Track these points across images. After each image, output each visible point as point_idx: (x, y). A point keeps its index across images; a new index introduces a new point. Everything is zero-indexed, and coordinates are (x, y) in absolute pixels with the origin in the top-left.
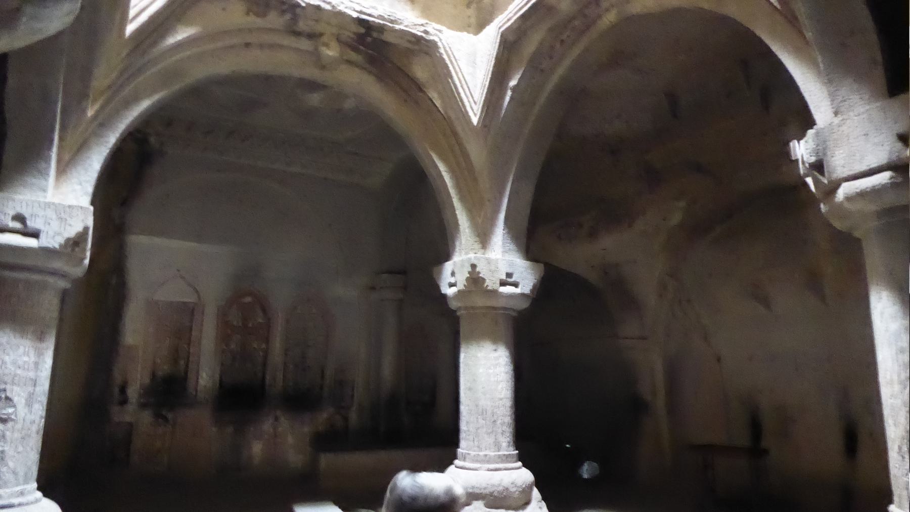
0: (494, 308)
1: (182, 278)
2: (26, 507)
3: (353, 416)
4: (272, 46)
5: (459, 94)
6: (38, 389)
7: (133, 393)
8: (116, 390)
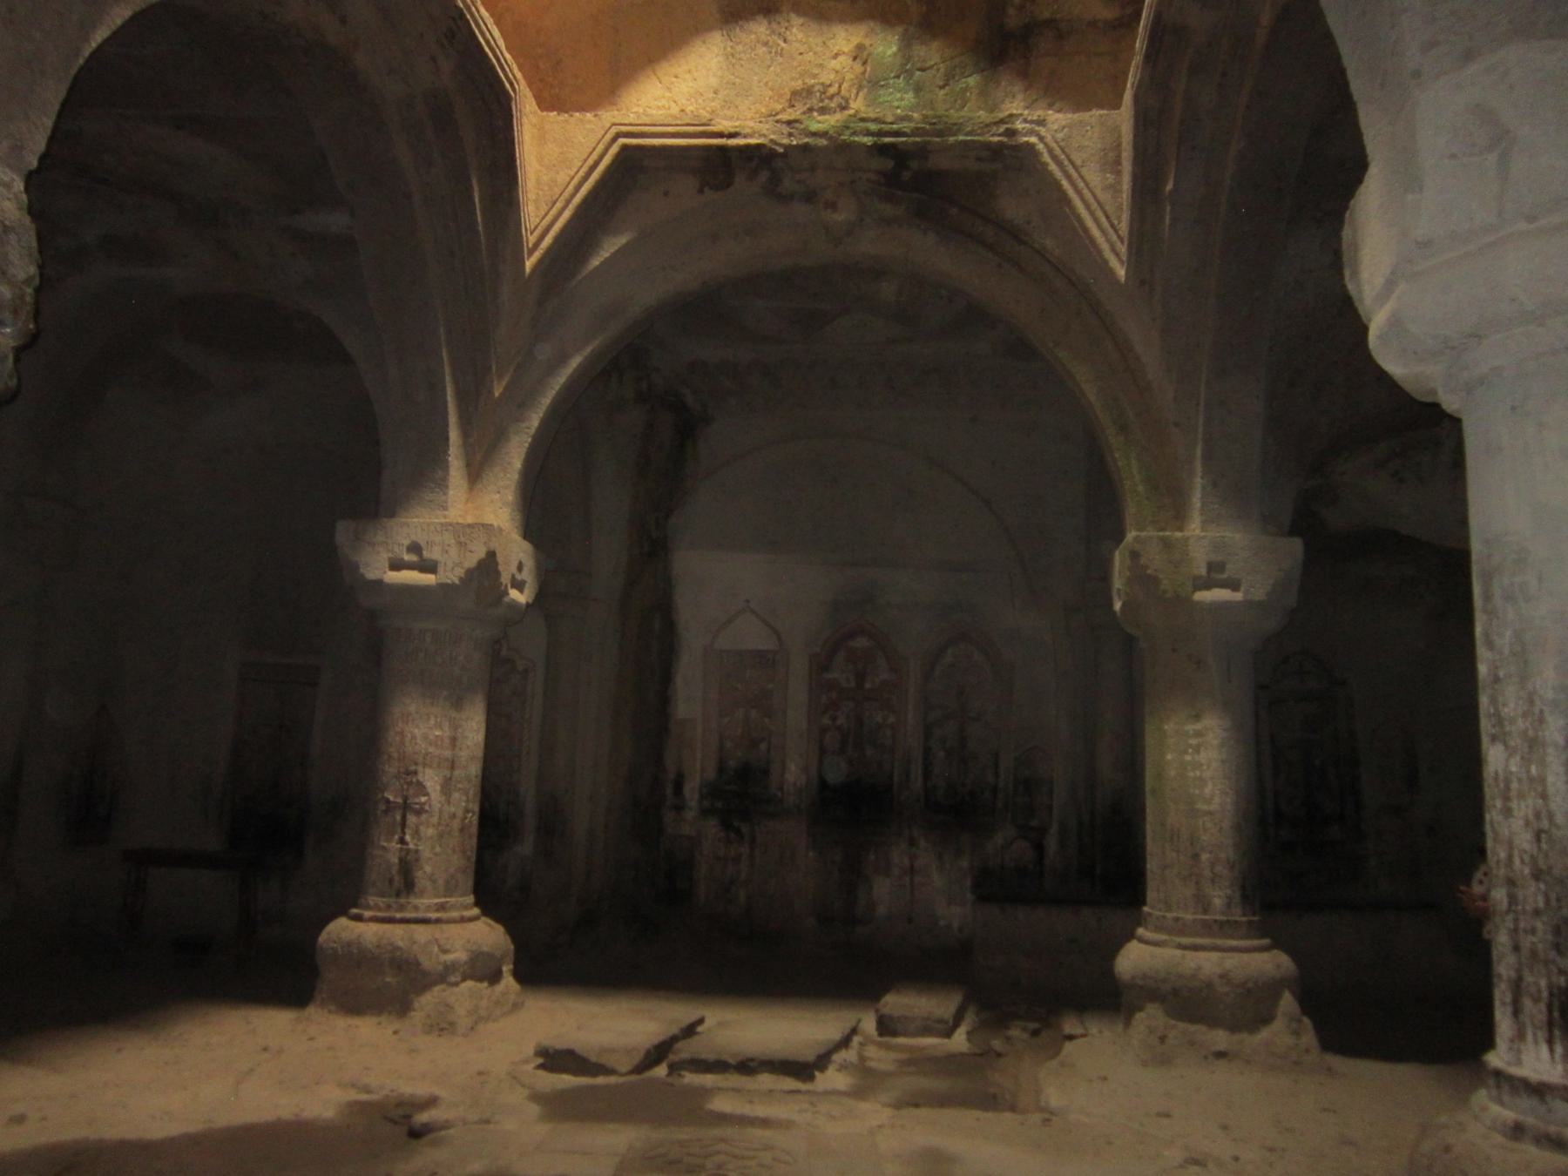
1: (753, 612)
2: (445, 927)
5: (1086, 230)
6: (457, 773)
7: (691, 791)
8: (669, 791)
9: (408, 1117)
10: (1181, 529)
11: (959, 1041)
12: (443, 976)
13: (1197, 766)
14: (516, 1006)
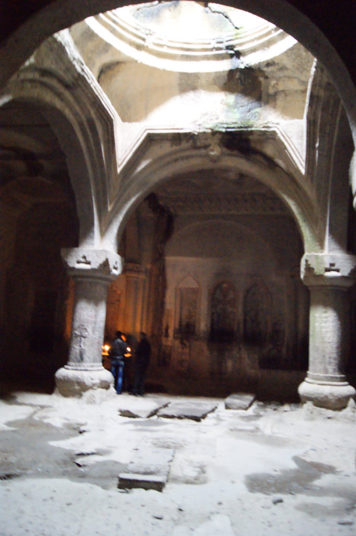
0: (323, 286)
3: (284, 350)
4: (188, 157)
5: (292, 157)
7: (171, 332)
8: (164, 331)
9: (79, 428)
10: (322, 252)
11: (250, 411)
12: (91, 388)
13: (324, 327)
14: (114, 397)
